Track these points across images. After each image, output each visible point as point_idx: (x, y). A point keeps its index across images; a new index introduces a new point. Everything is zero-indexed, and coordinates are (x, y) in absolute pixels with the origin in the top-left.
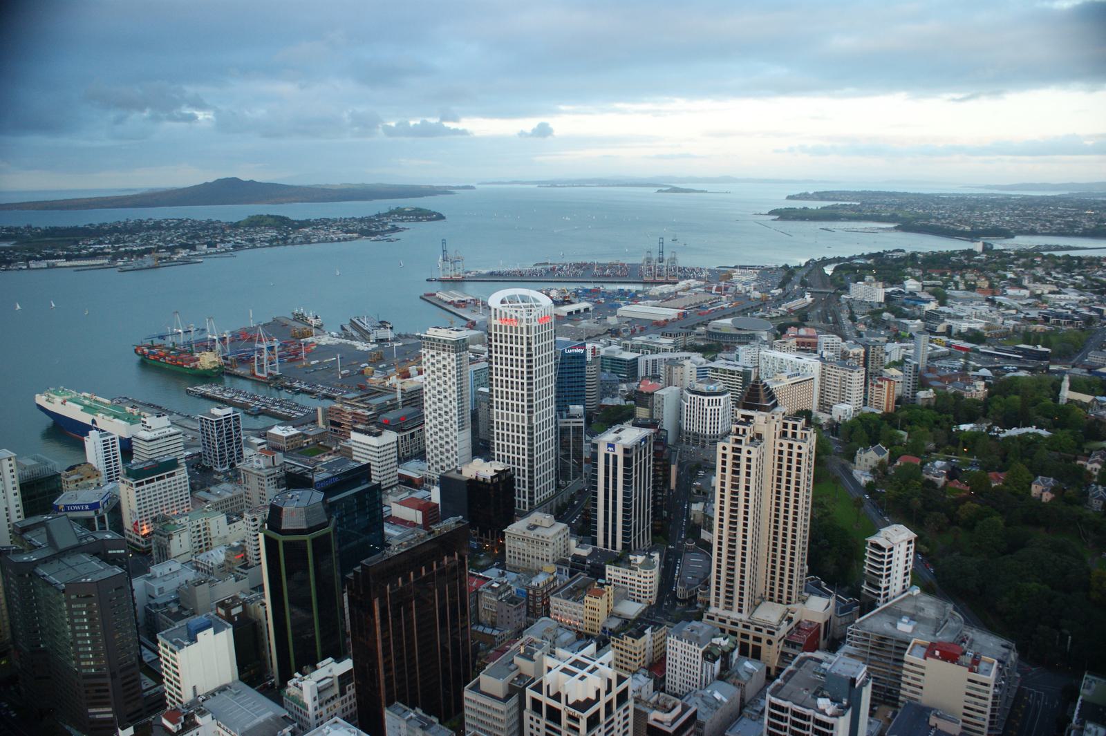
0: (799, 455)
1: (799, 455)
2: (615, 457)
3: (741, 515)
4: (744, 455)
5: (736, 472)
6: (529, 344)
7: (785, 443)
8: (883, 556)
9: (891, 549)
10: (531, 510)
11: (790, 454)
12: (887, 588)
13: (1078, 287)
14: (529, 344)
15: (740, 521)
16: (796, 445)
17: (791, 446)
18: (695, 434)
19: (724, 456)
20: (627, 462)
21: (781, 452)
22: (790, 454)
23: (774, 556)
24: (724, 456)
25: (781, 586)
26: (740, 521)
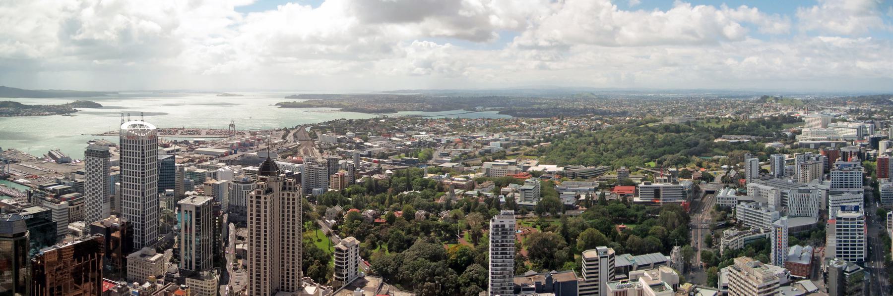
0: (294, 199)
1: (294, 199)
2: (191, 212)
3: (263, 233)
4: (262, 200)
5: (259, 211)
6: (143, 150)
7: (286, 193)
8: (343, 256)
9: (347, 251)
10: (143, 246)
11: (288, 199)
12: (347, 275)
13: (427, 132)
14: (143, 150)
15: (262, 241)
16: (291, 193)
17: (289, 195)
18: (237, 207)
19: (252, 202)
20: (198, 215)
21: (283, 199)
22: (288, 199)
23: (283, 255)
24: (252, 202)
25: (288, 281)
26: (262, 241)
